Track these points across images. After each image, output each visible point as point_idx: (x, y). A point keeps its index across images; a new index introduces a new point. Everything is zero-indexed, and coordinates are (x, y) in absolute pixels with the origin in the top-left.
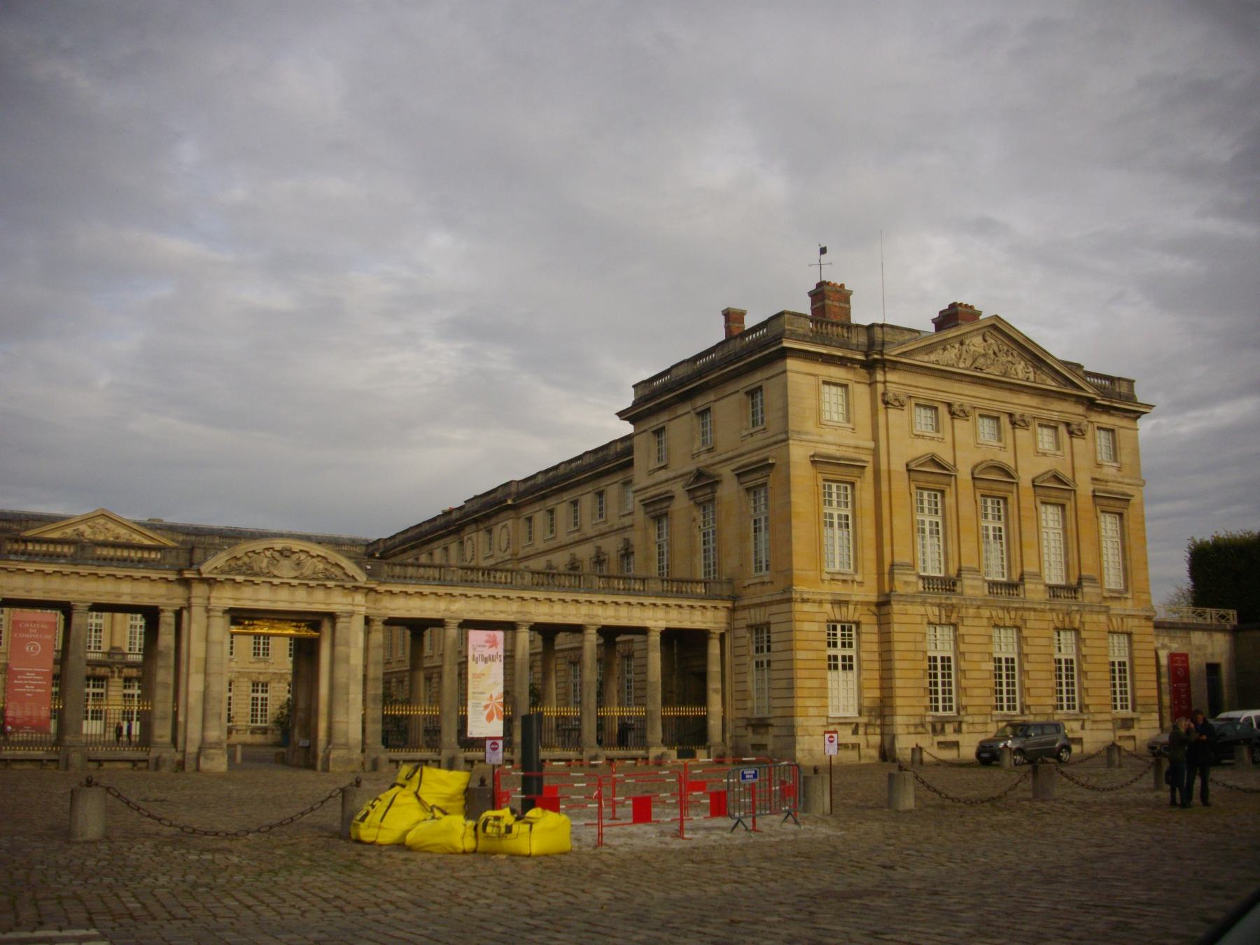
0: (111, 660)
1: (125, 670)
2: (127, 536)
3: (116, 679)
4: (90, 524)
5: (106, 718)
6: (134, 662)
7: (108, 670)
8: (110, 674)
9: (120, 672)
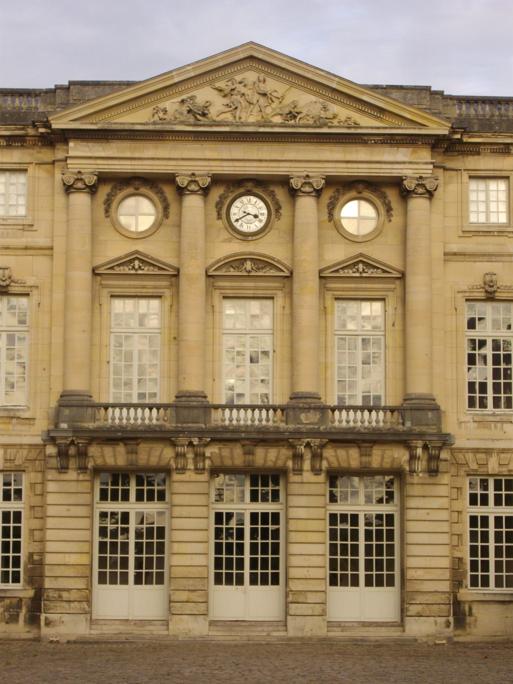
0: (291, 427)
1: (329, 453)
2: (316, 110)
3: (308, 476)
4: (221, 84)
5: (287, 579)
6: (351, 431)
7: (285, 452)
8: (290, 464)
9: (317, 456)
